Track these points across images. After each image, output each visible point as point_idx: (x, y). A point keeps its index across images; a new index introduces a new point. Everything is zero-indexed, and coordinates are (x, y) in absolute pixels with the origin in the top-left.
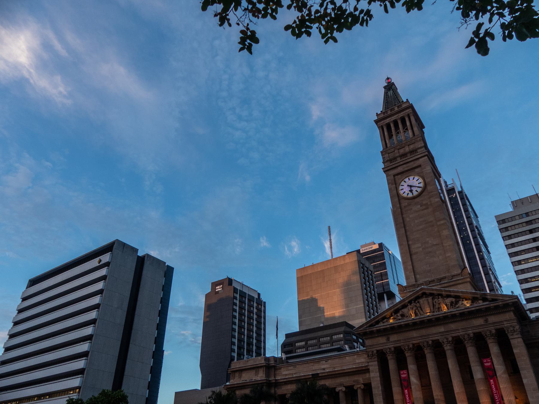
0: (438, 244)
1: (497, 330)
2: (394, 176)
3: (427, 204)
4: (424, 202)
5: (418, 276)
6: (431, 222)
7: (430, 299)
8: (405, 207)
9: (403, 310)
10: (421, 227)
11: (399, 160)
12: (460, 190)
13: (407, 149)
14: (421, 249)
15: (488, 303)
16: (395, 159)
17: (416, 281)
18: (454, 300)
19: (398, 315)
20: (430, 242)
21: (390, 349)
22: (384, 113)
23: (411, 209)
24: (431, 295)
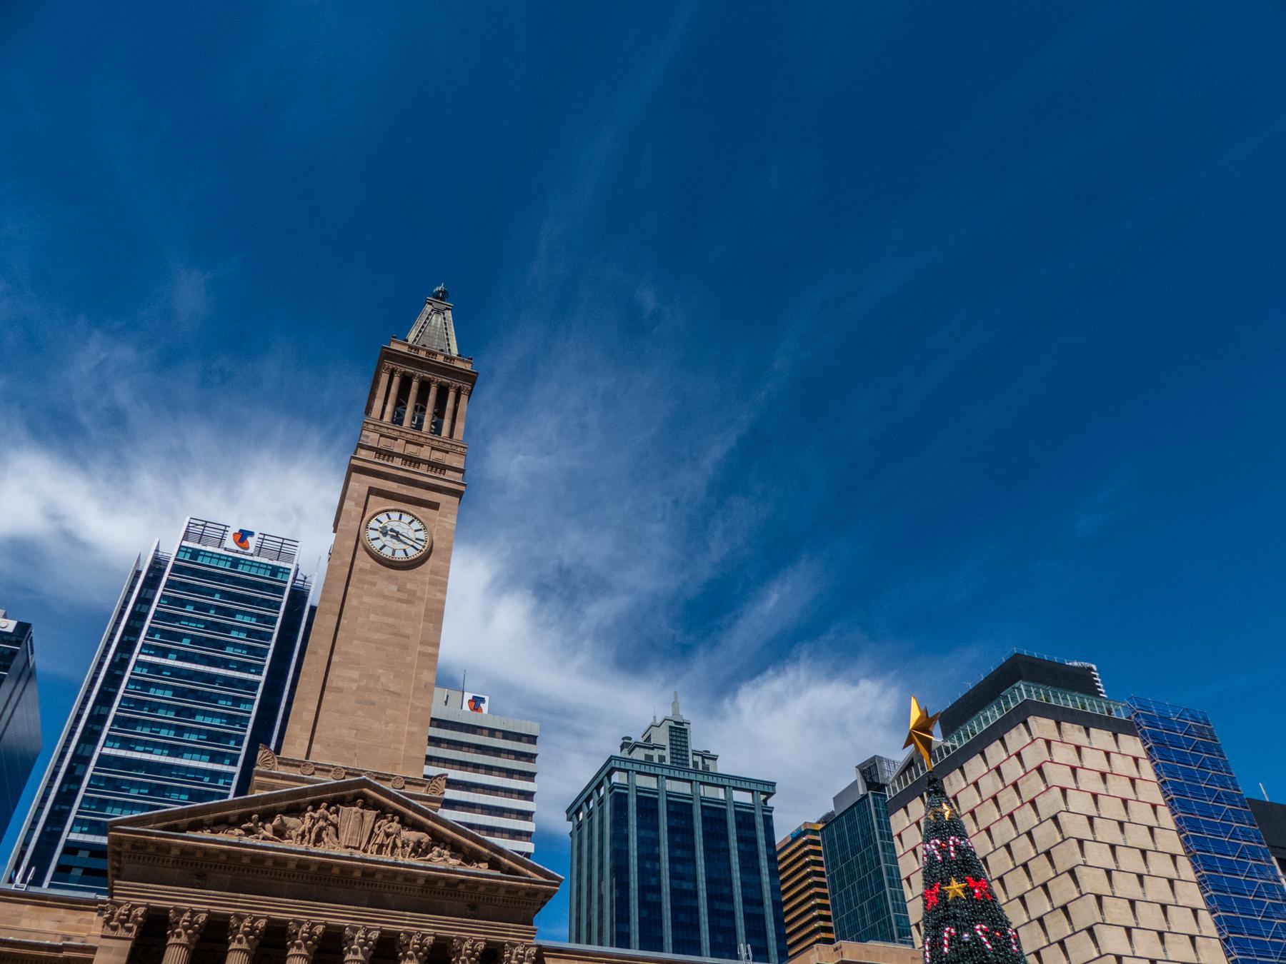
0: (398, 694)
1: (488, 943)
2: (372, 491)
3: (413, 593)
4: (409, 586)
5: (315, 747)
6: (407, 637)
7: (370, 815)
8: (361, 570)
9: (285, 818)
10: (378, 636)
11: (398, 462)
12: (316, 603)
13: (425, 453)
14: (354, 686)
15: (498, 873)
16: (390, 455)
17: (307, 757)
18: (426, 838)
19: (268, 826)
20: (383, 680)
21: (194, 913)
22: (411, 347)
23: (374, 584)
24: (376, 805)
